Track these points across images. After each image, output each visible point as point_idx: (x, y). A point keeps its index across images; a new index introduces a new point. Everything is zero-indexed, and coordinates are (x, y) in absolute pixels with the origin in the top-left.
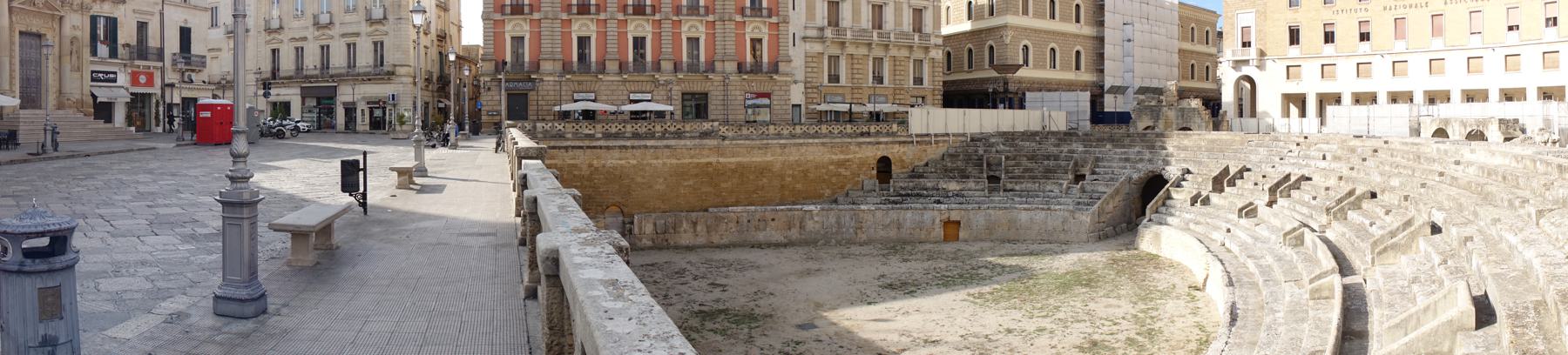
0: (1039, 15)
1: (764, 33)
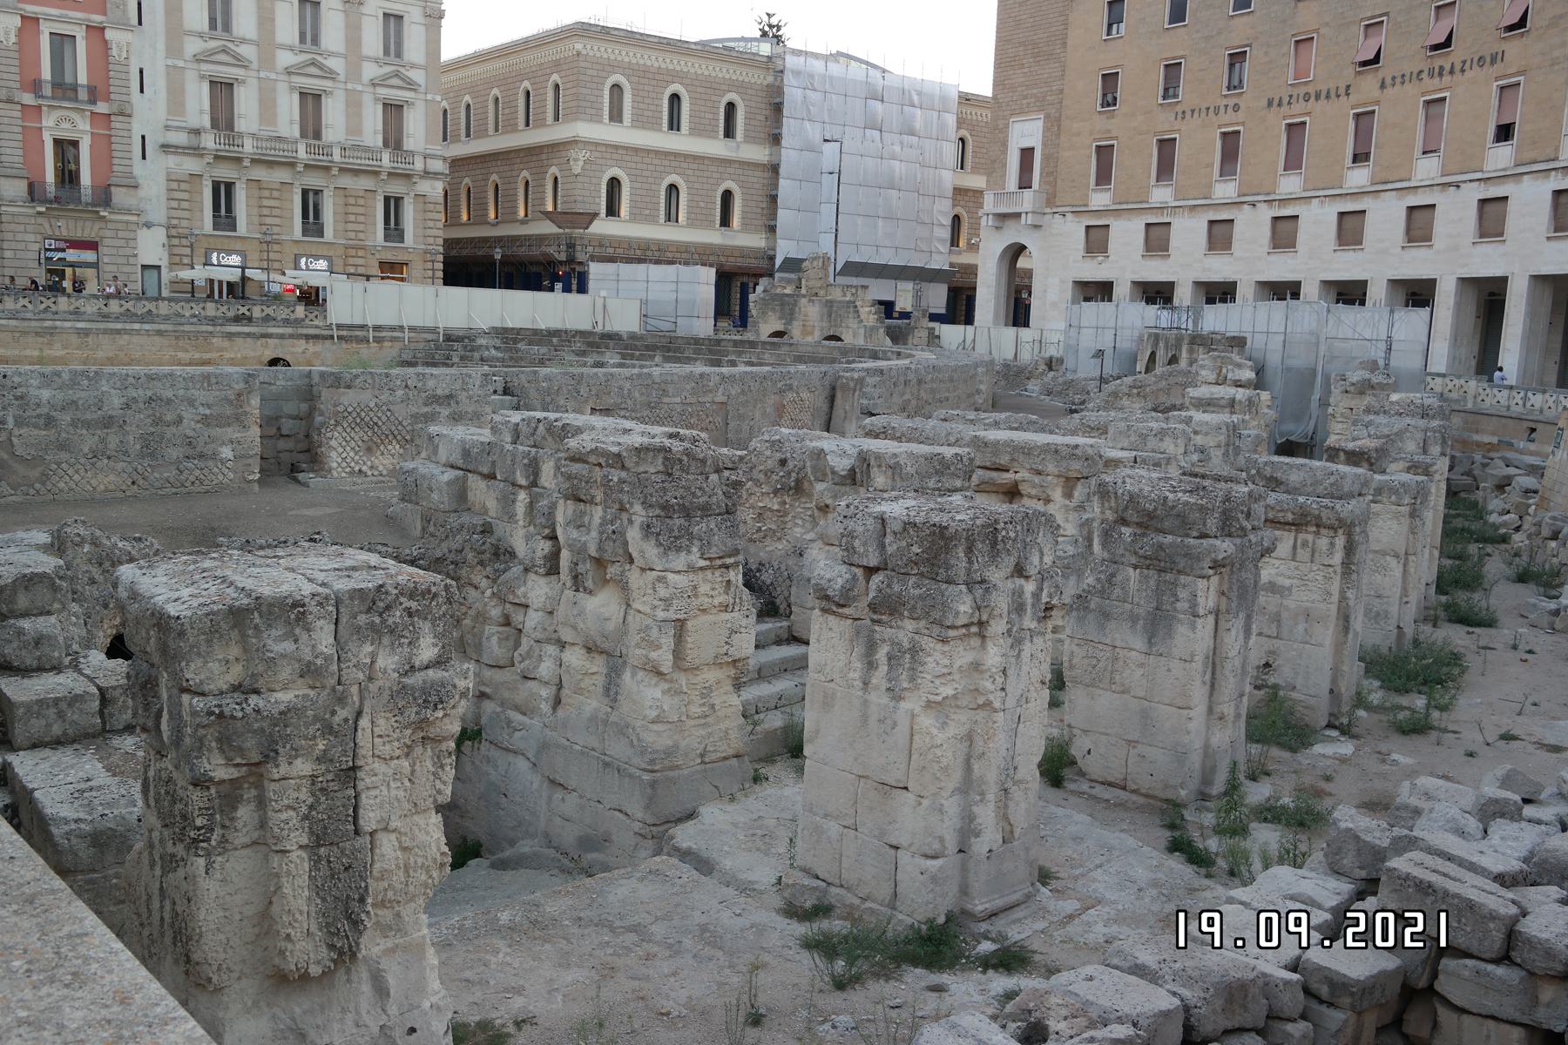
0: (640, 122)
1: (81, 128)
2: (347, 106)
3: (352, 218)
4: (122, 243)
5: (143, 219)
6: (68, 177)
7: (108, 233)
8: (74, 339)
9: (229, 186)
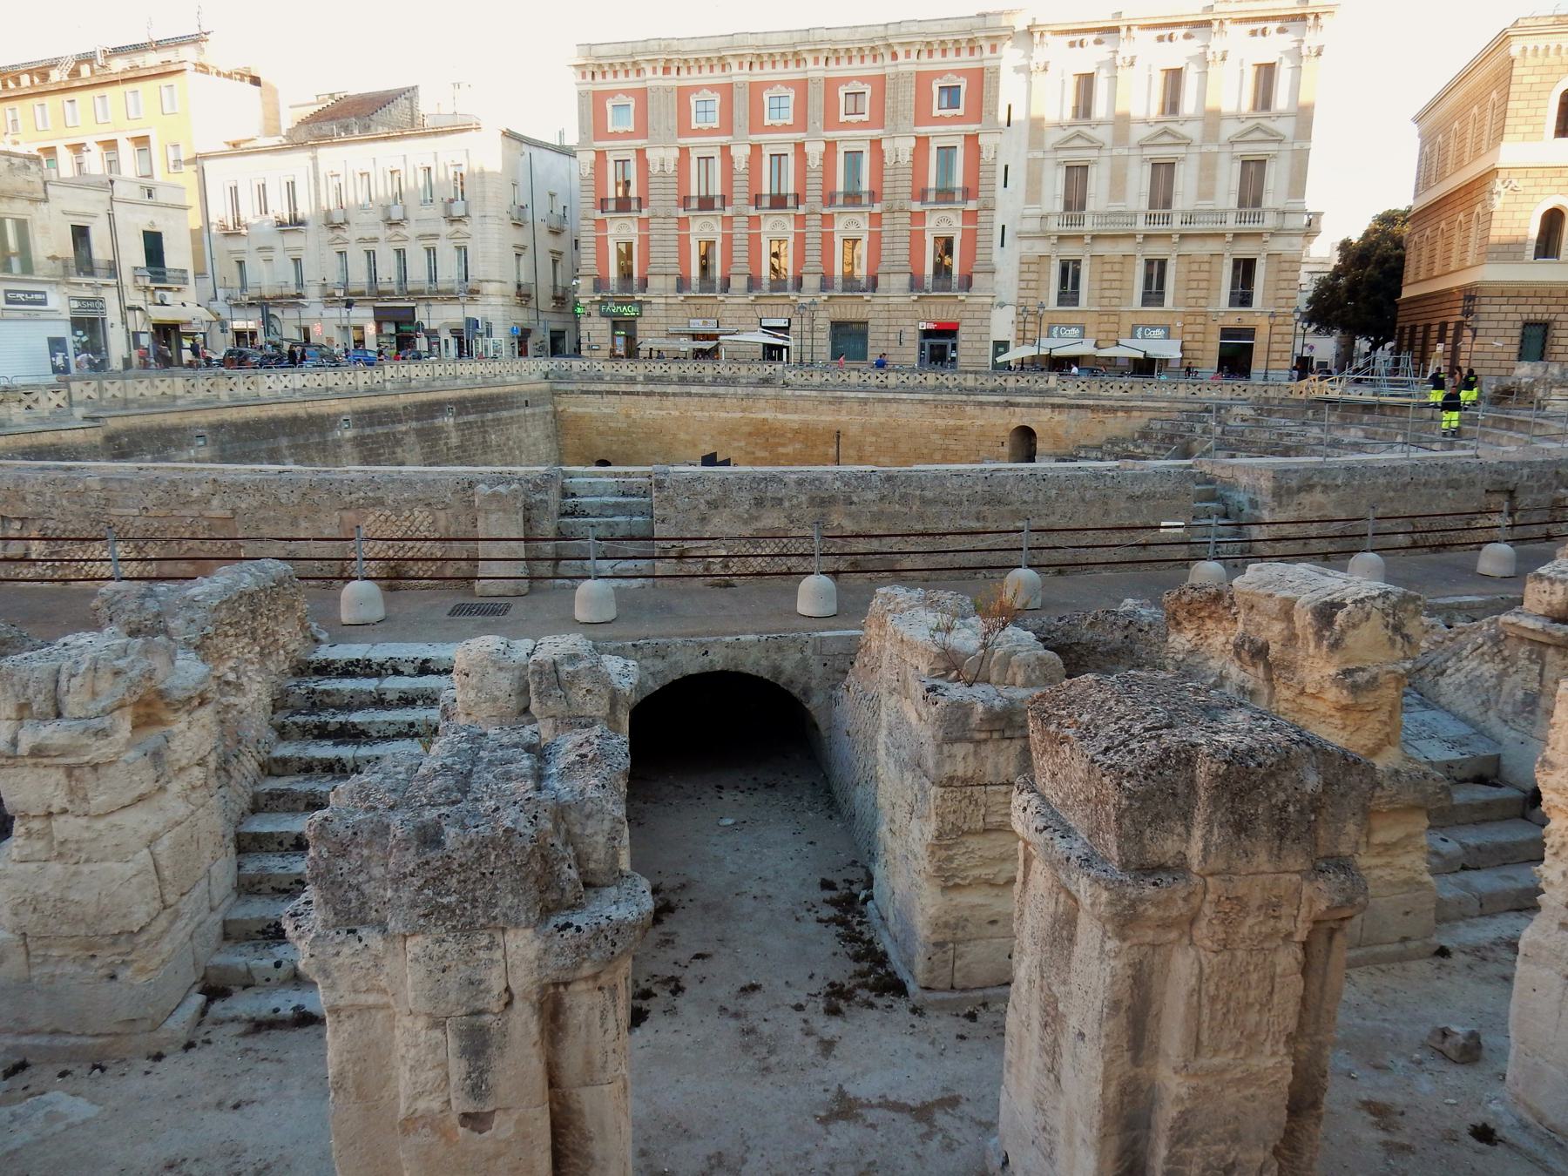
2: (1201, 169)
3: (1194, 285)
4: (977, 322)
5: (997, 301)
6: (942, 270)
7: (967, 315)
8: (856, 407)
9: (1163, 264)
